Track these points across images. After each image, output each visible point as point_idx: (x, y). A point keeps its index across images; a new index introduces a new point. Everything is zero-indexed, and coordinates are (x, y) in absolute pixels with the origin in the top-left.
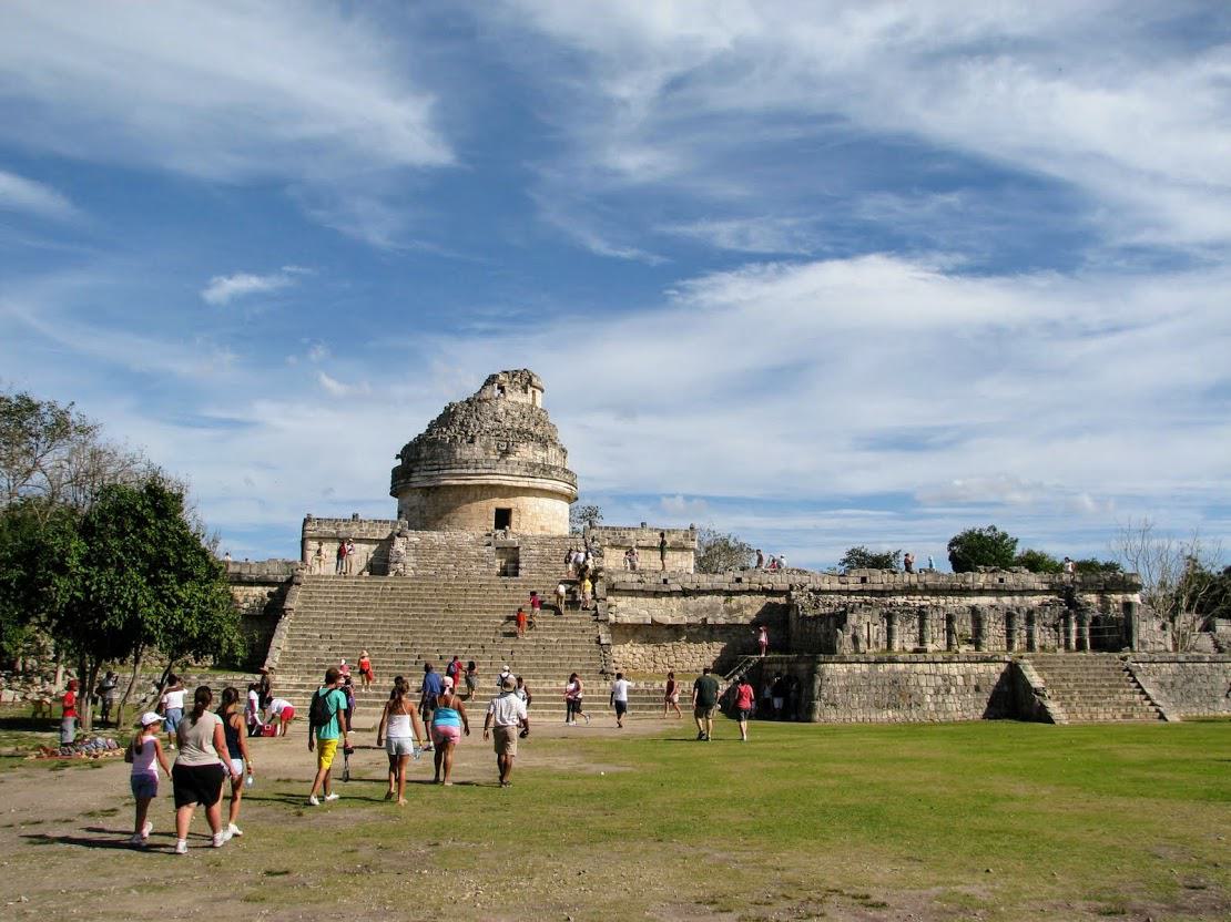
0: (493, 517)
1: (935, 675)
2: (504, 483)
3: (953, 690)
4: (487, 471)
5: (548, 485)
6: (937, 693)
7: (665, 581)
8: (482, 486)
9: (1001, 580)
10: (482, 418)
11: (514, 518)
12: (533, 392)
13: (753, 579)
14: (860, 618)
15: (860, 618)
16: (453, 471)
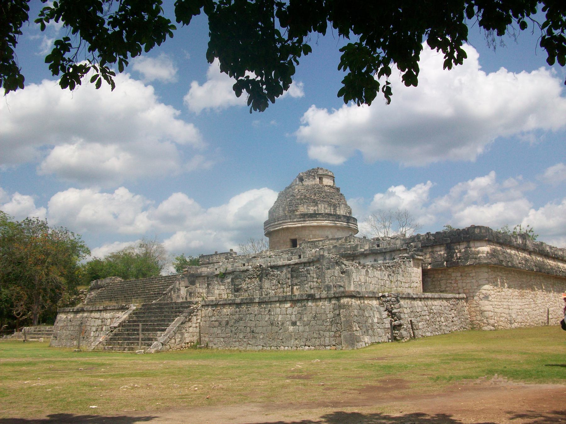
0: (289, 243)
1: (98, 318)
2: (289, 226)
3: (104, 328)
4: (284, 221)
5: (315, 223)
6: (97, 331)
7: (216, 269)
8: (283, 229)
9: (378, 246)
10: (287, 197)
11: (298, 243)
12: (321, 179)
13: (250, 264)
14: (180, 283)
15: (180, 283)
16: (272, 224)
